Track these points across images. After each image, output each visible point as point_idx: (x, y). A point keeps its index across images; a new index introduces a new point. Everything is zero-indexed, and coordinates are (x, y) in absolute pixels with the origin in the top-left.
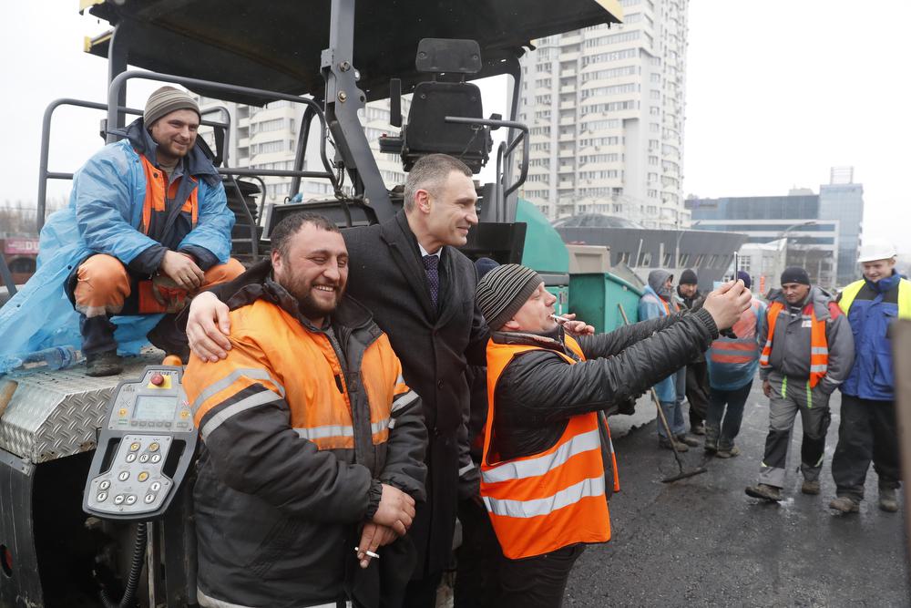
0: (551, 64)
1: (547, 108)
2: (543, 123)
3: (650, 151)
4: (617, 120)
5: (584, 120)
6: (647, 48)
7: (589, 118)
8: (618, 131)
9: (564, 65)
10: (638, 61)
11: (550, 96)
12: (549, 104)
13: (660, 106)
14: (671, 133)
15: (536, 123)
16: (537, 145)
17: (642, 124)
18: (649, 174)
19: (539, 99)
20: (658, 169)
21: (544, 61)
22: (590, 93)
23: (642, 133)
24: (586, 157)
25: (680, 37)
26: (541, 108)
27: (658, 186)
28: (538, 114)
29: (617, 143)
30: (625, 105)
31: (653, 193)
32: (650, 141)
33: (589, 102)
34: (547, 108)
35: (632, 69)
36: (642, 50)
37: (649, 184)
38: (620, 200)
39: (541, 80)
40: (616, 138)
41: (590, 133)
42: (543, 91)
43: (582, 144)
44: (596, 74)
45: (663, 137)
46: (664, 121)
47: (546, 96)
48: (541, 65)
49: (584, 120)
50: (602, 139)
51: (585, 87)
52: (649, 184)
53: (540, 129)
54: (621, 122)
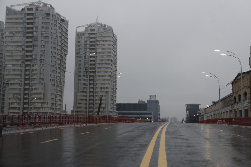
0: (87, 76)
1: (86, 86)
2: (85, 90)
3: (111, 98)
4: (104, 91)
5: (96, 90)
6: (111, 75)
7: (97, 90)
8: (105, 94)
9: (90, 76)
10: (109, 78)
11: (87, 83)
12: (87, 86)
13: (113, 87)
14: (115, 93)
15: (83, 90)
16: (83, 95)
17: (110, 92)
18: (111, 104)
19: (84, 84)
20: (112, 102)
21: (85, 75)
22: (98, 84)
23: (110, 94)
24: (96, 99)
25: (116, 70)
26: (84, 86)
27: (112, 106)
28: (84, 88)
29: (104, 96)
30: (106, 88)
31: (112, 108)
32: (111, 96)
33: (97, 86)
34: (86, 86)
35: (108, 80)
36: (110, 75)
37: (111, 106)
38: (105, 110)
39: (85, 79)
40: (104, 95)
41: (98, 93)
42: (85, 82)
43: (95, 96)
44: (99, 80)
45: (114, 95)
46: (114, 90)
47: (86, 83)
48: (85, 76)
49: (96, 90)
50: (101, 95)
51: (96, 82)
52: (111, 106)
53: (84, 91)
54: (105, 92)
